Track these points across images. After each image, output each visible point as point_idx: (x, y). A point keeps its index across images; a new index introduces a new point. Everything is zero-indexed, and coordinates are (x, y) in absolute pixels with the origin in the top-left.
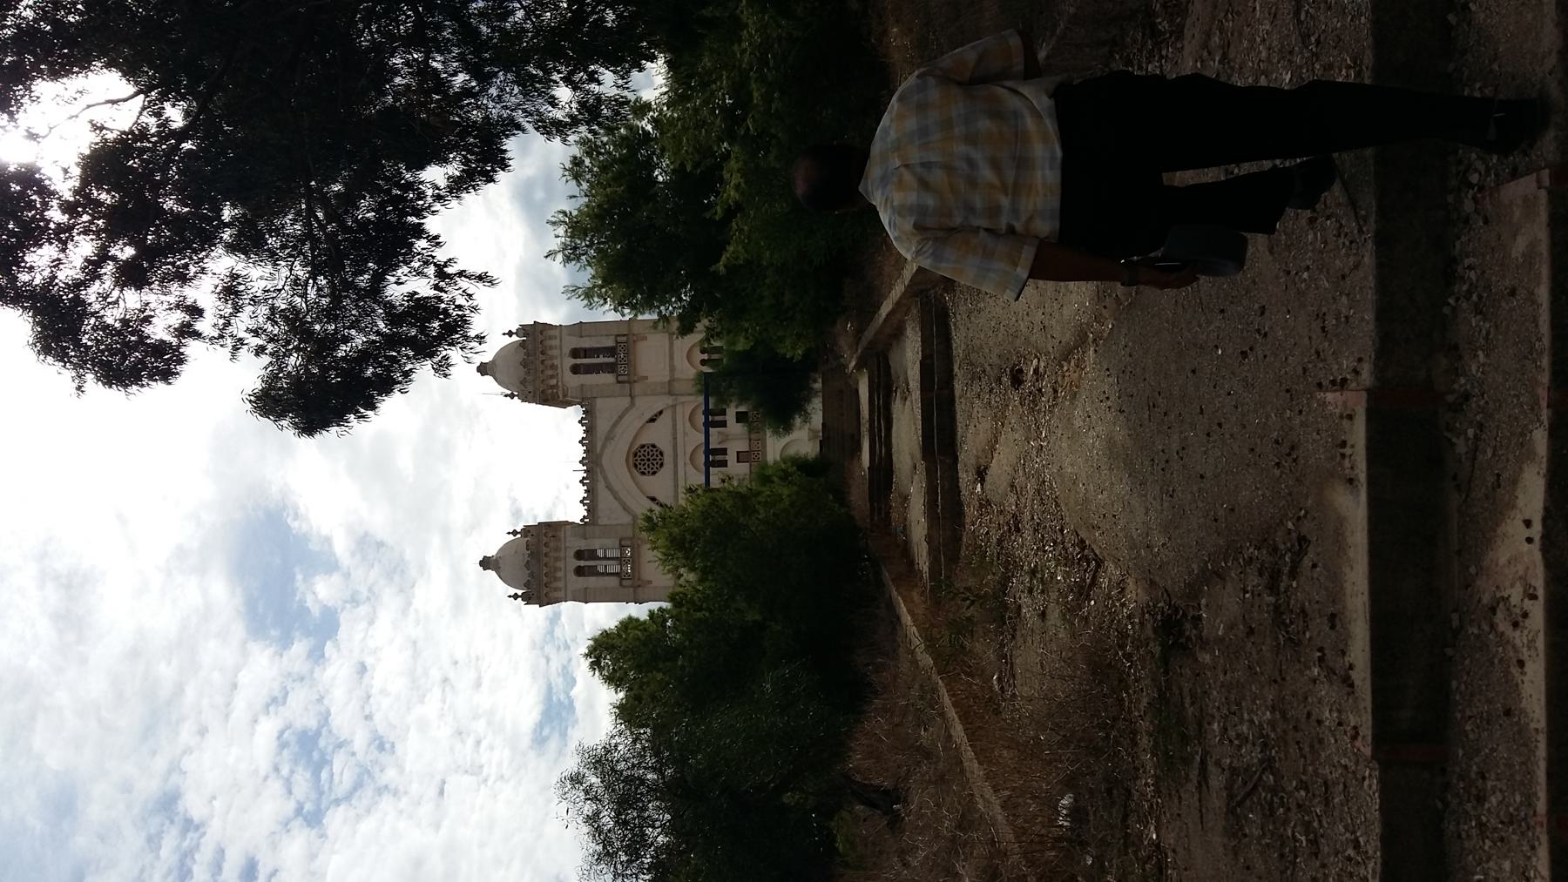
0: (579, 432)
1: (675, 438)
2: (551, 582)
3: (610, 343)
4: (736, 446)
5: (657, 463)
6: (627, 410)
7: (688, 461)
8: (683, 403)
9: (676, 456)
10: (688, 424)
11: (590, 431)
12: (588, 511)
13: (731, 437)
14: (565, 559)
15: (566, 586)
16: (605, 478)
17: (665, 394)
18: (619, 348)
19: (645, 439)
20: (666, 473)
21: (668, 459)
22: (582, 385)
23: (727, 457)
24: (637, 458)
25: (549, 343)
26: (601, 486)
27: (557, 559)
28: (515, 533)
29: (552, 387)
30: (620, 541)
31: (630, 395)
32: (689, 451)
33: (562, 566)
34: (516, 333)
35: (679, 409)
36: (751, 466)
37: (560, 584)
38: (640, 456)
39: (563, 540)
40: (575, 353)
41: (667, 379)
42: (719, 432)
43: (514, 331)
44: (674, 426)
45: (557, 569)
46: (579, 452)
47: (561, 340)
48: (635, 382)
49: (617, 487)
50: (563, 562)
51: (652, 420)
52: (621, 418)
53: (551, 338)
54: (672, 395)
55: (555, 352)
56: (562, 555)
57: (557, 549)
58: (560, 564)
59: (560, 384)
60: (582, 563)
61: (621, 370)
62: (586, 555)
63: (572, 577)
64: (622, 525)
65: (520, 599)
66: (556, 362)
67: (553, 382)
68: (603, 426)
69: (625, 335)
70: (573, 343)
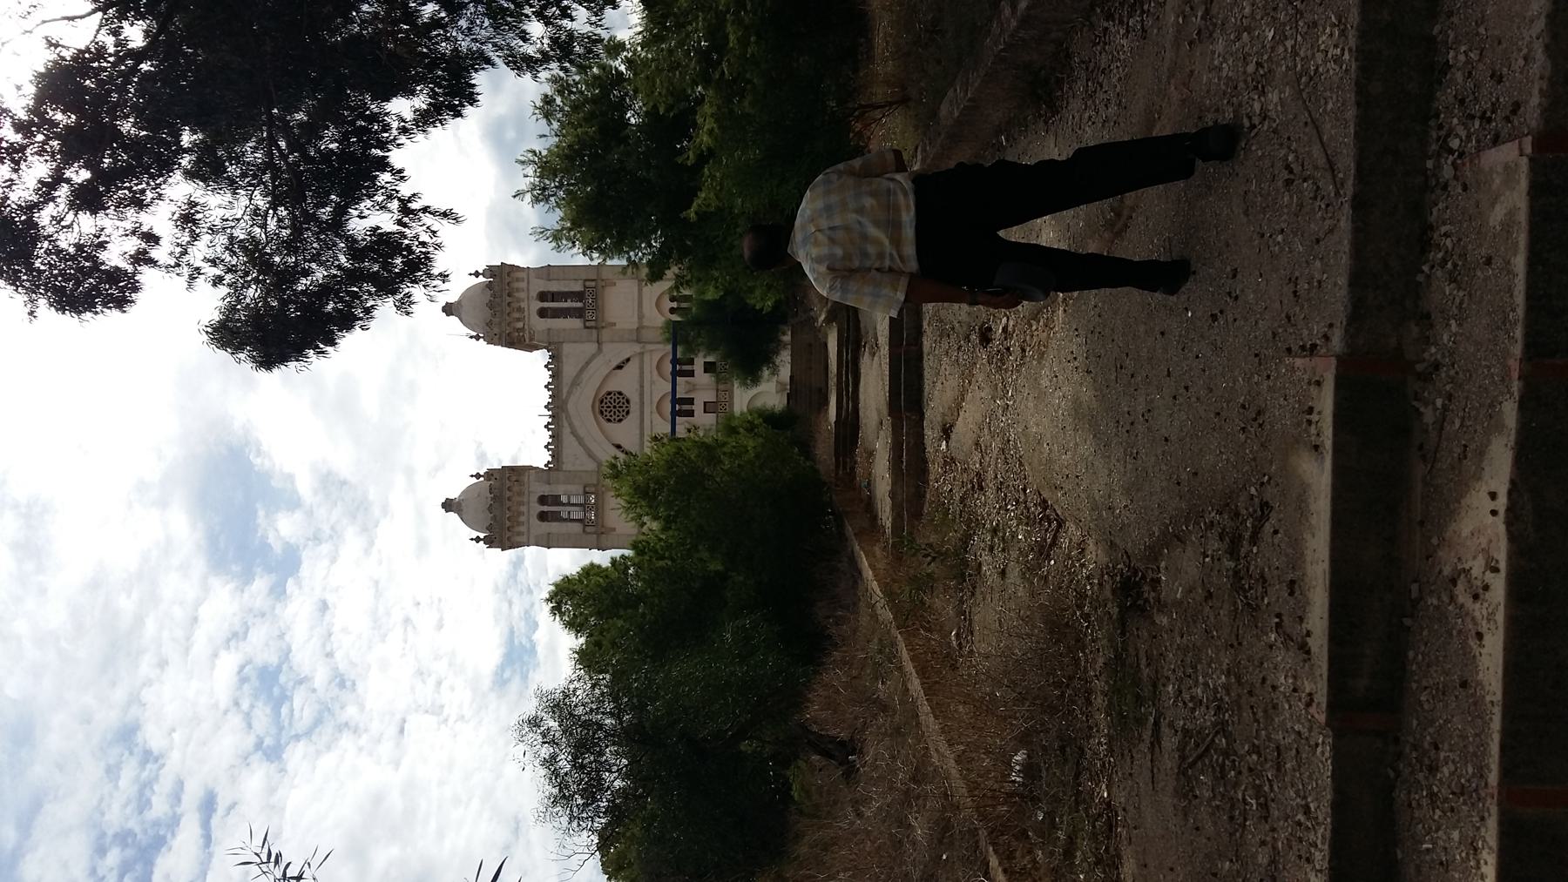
0: (545, 376)
1: (642, 387)
2: (513, 527)
3: (578, 287)
4: (701, 398)
6: (593, 357)
8: (651, 351)
9: (642, 404)
10: (655, 373)
11: (556, 375)
12: (553, 456)
15: (529, 531)
16: (571, 425)
17: (633, 341)
19: (612, 386)
20: (631, 422)
21: (634, 407)
22: (549, 329)
23: (694, 407)
25: (516, 285)
26: (566, 431)
27: (521, 503)
28: (478, 476)
29: (518, 330)
30: (585, 488)
31: (598, 342)
32: (656, 400)
34: (483, 274)
35: (647, 358)
37: (523, 529)
39: (526, 486)
40: (543, 296)
41: (635, 326)
42: (687, 382)
43: (481, 272)
45: (520, 514)
46: (545, 397)
47: (528, 283)
48: (603, 327)
49: (582, 433)
51: (619, 367)
52: (588, 363)
53: (518, 280)
54: (640, 343)
55: (522, 295)
56: (525, 500)
57: (520, 494)
58: (524, 509)
59: (526, 327)
60: (546, 508)
61: (588, 315)
62: (550, 501)
63: (535, 521)
64: (586, 471)
65: (482, 542)
66: (524, 305)
67: (520, 325)
68: (569, 371)
70: (540, 285)
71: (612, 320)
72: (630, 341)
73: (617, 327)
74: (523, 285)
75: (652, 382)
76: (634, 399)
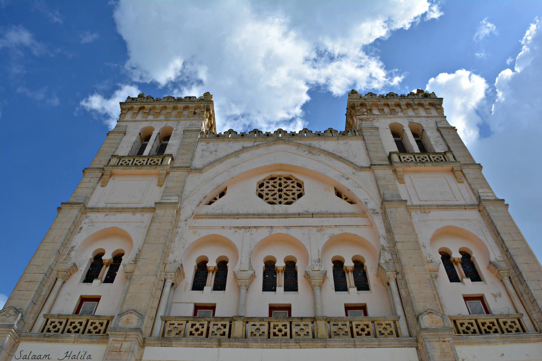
1: (313, 215)
7: (275, 231)
9: (287, 216)
32: (296, 233)
35: (360, 221)
36: (262, 319)
42: (325, 274)
44: (334, 215)
49: (245, 156)
63: (145, 125)
71: (407, 179)
75: (320, 228)
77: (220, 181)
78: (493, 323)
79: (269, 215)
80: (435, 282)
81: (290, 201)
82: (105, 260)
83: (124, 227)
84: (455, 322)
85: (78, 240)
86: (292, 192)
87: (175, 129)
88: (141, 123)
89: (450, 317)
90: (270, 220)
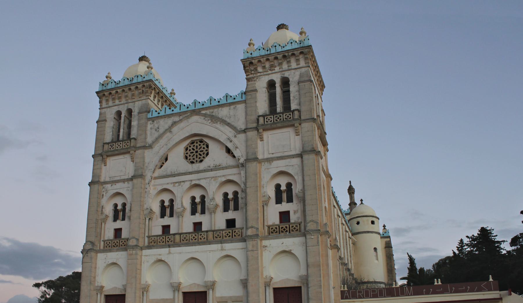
3: (293, 106)
4: (204, 219)
5: (200, 158)
7: (194, 182)
10: (224, 179)
13: (213, 215)
14: (127, 103)
15: (109, 107)
16: (181, 121)
18: (278, 116)
19: (213, 148)
20: (187, 167)
21: (197, 166)
24: (199, 143)
25: (293, 60)
29: (256, 69)
32: (202, 183)
33: (122, 102)
38: (200, 145)
48: (258, 131)
49: (175, 129)
50: (125, 102)
51: (228, 151)
52: (228, 124)
55: (285, 66)
58: (123, 101)
59: (259, 74)
61: (271, 118)
63: (116, 109)
66: (277, 69)
68: (223, 113)
69: (300, 117)
72: (247, 153)
73: (259, 143)
74: (294, 65)
76: (202, 166)
77: (162, 152)
78: (286, 227)
79: (189, 172)
80: (265, 207)
81: (202, 159)
82: (119, 209)
83: (121, 191)
84: (269, 227)
85: (104, 201)
86: (203, 152)
87: (133, 111)
88: (113, 108)
89: (266, 226)
90: (190, 175)
